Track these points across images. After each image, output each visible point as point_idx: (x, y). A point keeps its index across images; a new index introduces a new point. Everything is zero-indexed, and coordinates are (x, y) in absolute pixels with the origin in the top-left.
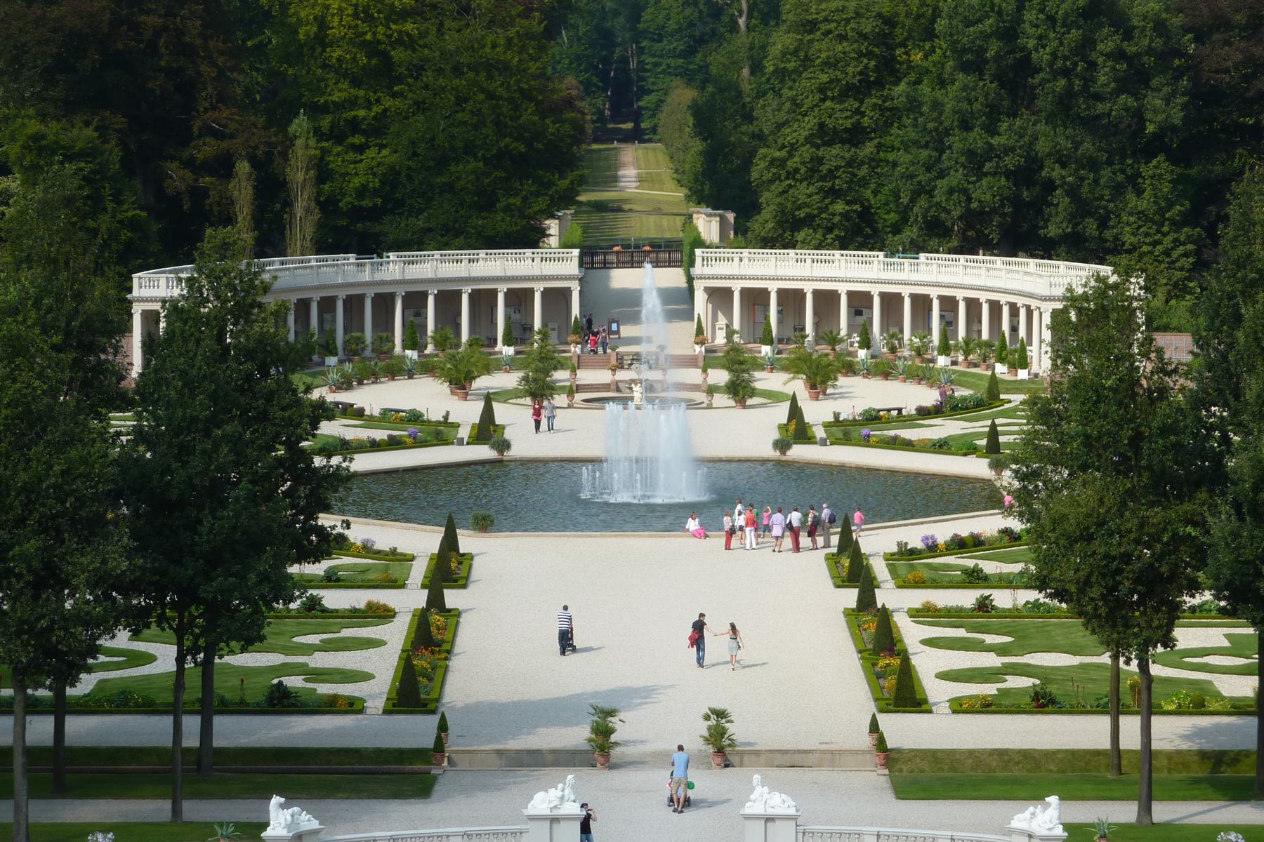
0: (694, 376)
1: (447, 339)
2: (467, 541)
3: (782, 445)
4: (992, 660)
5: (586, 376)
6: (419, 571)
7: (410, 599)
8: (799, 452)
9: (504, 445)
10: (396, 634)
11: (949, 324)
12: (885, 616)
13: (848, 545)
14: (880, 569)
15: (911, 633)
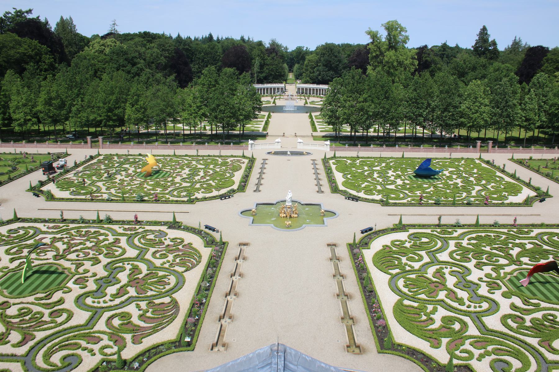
0: (296, 97)
1: (271, 93)
2: (271, 114)
3: (305, 104)
4: (324, 127)
5: (285, 97)
6: (266, 117)
7: (266, 119)
8: (306, 105)
9: (276, 104)
10: (263, 123)
12: (314, 122)
13: (311, 115)
15: (316, 124)
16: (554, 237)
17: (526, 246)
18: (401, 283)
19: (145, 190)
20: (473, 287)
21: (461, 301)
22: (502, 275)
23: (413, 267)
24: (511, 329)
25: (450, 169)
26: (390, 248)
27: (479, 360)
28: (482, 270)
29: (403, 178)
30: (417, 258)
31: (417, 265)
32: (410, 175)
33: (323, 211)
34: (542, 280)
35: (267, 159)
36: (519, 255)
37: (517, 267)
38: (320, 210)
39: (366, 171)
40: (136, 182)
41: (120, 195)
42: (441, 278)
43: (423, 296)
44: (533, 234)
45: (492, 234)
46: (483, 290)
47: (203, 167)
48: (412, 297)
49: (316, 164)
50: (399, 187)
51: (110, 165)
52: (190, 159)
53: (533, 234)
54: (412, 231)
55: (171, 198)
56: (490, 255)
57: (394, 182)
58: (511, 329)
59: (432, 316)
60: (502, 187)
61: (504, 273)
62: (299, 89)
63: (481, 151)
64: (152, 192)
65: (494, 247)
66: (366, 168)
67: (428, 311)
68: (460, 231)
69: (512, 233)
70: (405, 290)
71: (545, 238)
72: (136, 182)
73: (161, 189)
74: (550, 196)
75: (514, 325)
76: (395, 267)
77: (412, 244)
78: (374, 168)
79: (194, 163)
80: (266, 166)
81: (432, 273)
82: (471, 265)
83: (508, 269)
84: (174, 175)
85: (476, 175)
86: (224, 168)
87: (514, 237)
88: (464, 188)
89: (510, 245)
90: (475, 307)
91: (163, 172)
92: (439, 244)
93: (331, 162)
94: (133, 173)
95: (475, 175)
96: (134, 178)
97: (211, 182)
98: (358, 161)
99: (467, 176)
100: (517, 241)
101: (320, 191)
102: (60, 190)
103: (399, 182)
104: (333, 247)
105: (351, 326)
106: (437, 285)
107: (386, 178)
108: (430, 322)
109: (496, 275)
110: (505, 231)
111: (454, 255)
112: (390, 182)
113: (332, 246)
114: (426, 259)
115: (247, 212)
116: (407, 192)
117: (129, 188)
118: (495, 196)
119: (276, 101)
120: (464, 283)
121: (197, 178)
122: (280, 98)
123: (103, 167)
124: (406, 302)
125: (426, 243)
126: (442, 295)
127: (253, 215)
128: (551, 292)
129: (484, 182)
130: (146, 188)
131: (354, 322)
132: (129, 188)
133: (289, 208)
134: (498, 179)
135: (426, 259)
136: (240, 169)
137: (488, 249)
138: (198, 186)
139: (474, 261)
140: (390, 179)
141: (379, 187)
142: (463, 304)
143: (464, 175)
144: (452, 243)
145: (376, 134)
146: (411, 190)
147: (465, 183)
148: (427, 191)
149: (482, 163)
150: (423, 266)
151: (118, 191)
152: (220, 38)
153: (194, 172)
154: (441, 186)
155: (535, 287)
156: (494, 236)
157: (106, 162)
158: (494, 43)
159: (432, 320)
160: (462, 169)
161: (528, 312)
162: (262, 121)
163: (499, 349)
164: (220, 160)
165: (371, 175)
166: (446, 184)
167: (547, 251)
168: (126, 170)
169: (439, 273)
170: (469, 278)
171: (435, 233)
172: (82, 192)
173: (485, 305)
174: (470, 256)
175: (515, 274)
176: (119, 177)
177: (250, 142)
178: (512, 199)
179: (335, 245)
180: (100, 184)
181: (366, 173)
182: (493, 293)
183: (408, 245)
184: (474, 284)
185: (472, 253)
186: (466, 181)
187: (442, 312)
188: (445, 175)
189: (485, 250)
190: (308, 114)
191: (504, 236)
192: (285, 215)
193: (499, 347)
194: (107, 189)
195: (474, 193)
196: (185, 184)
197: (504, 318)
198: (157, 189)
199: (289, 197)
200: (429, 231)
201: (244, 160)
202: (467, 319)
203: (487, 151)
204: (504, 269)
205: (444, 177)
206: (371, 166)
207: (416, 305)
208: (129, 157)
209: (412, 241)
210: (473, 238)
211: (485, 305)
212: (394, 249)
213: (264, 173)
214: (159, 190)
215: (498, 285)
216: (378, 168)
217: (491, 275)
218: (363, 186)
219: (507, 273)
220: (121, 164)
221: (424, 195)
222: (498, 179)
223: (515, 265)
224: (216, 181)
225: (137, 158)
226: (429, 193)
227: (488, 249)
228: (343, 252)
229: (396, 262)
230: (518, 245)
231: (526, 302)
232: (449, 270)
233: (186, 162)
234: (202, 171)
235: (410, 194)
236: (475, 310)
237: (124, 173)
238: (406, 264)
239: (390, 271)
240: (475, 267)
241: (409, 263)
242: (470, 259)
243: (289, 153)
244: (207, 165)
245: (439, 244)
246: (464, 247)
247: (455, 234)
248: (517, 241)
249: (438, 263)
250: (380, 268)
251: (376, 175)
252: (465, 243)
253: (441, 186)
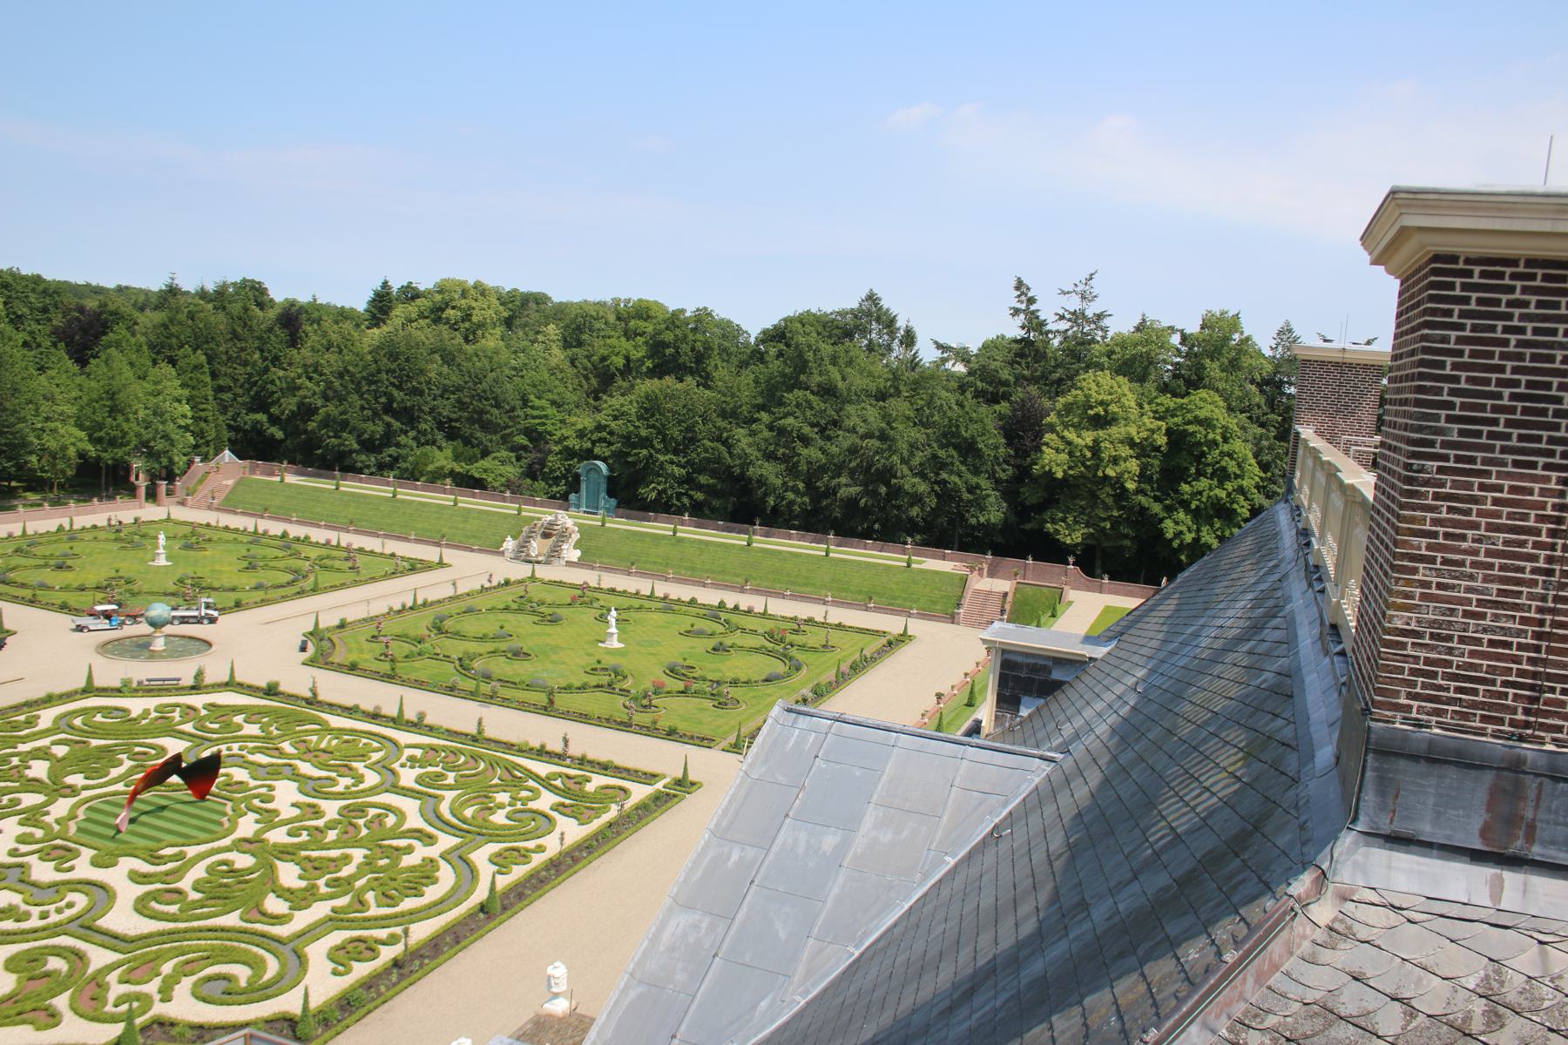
24: (172, 918)
27: (166, 998)
34: (148, 808)
36: (55, 775)
37: (75, 799)
58: (172, 918)
128: (182, 823)
155: (144, 824)
161: (177, 874)
163: (187, 962)
175: (81, 816)
182: (72, 869)
184: (9, 867)
193: (181, 958)
197: (141, 907)
215: (69, 850)
217: (32, 835)
219: (63, 818)
231: (155, 859)
236: (61, 917)
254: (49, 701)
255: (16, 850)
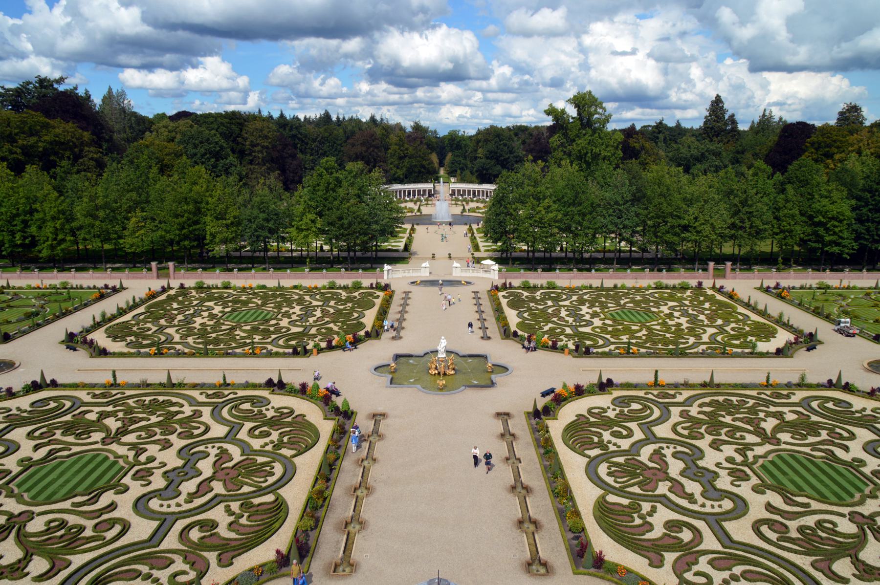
2: (415, 227)
3: (462, 213)
6: (408, 231)
7: (407, 235)
8: (464, 214)
11: (487, 194)
12: (475, 238)
13: (471, 229)
14: (475, 231)
16: (828, 403)
17: (785, 416)
18: (603, 470)
19: (238, 337)
20: (709, 476)
21: (690, 498)
22: (751, 459)
23: (619, 447)
25: (671, 304)
26: (588, 418)
28: (721, 451)
29: (602, 316)
30: (625, 433)
31: (625, 444)
32: (613, 313)
33: (490, 365)
35: (410, 292)
36: (777, 429)
38: (486, 364)
39: (550, 307)
40: (224, 327)
41: (201, 346)
42: (661, 462)
43: (636, 490)
44: (794, 399)
45: (734, 399)
46: (724, 482)
47: (321, 303)
48: (619, 490)
49: (480, 298)
50: (598, 330)
51: (186, 303)
52: (301, 293)
53: (794, 399)
54: (617, 393)
55: (275, 350)
56: (733, 430)
57: (589, 323)
59: (649, 519)
60: (748, 329)
61: (754, 457)
62: (453, 191)
63: (715, 276)
64: (248, 341)
65: (737, 418)
66: (550, 303)
67: (644, 511)
68: (686, 394)
69: (763, 396)
70: (610, 480)
71: (814, 404)
72: (224, 327)
73: (261, 337)
74: (820, 343)
75: (773, 536)
76: (593, 445)
77: (617, 412)
78: (561, 303)
79: (307, 298)
80: (409, 302)
81: (648, 456)
82: (703, 443)
83: (760, 451)
84: (279, 316)
85: (708, 312)
86: (350, 305)
87: (767, 403)
88: (691, 331)
89: (762, 415)
90: (713, 507)
91: (262, 312)
92: (657, 413)
93: (500, 294)
94: (220, 315)
95: (706, 312)
96: (222, 321)
97: (331, 325)
98: (538, 293)
99: (695, 313)
100: (772, 409)
101: (485, 337)
102: (112, 341)
103: (597, 322)
104: (505, 417)
105: (533, 534)
106: (657, 472)
107: (578, 317)
108: (647, 527)
109: (742, 459)
110: (754, 393)
111: (679, 429)
112: (584, 323)
113: (504, 416)
114: (638, 435)
115: (382, 369)
116: (608, 337)
117: (214, 335)
118: (737, 342)
119: (421, 208)
120: (695, 470)
121: (311, 320)
122: (427, 204)
123: (175, 305)
124: (611, 498)
125: (636, 410)
126: (663, 488)
127: (391, 373)
128: (826, 486)
129: (719, 322)
130: (238, 335)
131: (536, 528)
132: (214, 335)
133: (442, 361)
134: (741, 317)
135: (638, 435)
136: (374, 305)
137: (728, 419)
138: (313, 331)
139: (709, 438)
140: (584, 318)
141: (568, 331)
142: (695, 502)
143: (690, 312)
144: (675, 411)
145: (563, 255)
146: (615, 333)
147: (693, 323)
148: (636, 335)
149: (716, 294)
150: (633, 445)
151: (197, 341)
152: (341, 117)
153: (308, 311)
154: (658, 327)
156: (737, 401)
157: (180, 298)
158: (733, 120)
159: (650, 527)
160: (687, 302)
162: (403, 238)
164: (344, 293)
165: (557, 313)
166: (664, 324)
167: (816, 423)
168: (210, 309)
169: (658, 455)
170: (701, 463)
171: (650, 396)
172: (145, 342)
173: (727, 504)
174: (702, 430)
175: (770, 458)
176: (199, 320)
177: (386, 267)
178: (762, 347)
179: (508, 414)
180: (171, 331)
181: (550, 311)
182: (739, 486)
183: (611, 414)
185: (704, 427)
186: (693, 320)
187: (663, 515)
188: (663, 312)
189: (722, 422)
190: (468, 227)
191: (751, 402)
192: (437, 372)
194: (181, 338)
195: (705, 338)
196: (295, 330)
198: (254, 336)
199: (442, 346)
200: (641, 393)
201: (378, 293)
202: (700, 524)
203: (724, 277)
204: (753, 450)
205: (662, 315)
206: (557, 299)
207: (625, 502)
208: (213, 291)
209: (618, 409)
210: (707, 403)
211: (727, 504)
212: (592, 419)
213: (406, 312)
214: (257, 338)
216: (567, 303)
217: (733, 459)
218: (546, 328)
220: (203, 301)
221: (634, 341)
222: (741, 317)
223: (770, 443)
224: (340, 324)
225: (225, 293)
226: (640, 338)
227: (728, 419)
228: (520, 426)
229: (596, 439)
230: (774, 415)
231: (788, 501)
232: (672, 450)
233: (296, 297)
234: (319, 310)
235: (612, 340)
237: (205, 314)
238: (609, 442)
239: (587, 452)
240: (710, 446)
241: (614, 440)
242: (702, 434)
243: (440, 282)
244: (326, 301)
245: (657, 413)
246: (692, 417)
247: (680, 399)
248: (772, 409)
249: (655, 440)
250: (572, 446)
251: (563, 313)
252: (694, 411)
253: (658, 327)
254: (802, 385)
255: (721, 464)
